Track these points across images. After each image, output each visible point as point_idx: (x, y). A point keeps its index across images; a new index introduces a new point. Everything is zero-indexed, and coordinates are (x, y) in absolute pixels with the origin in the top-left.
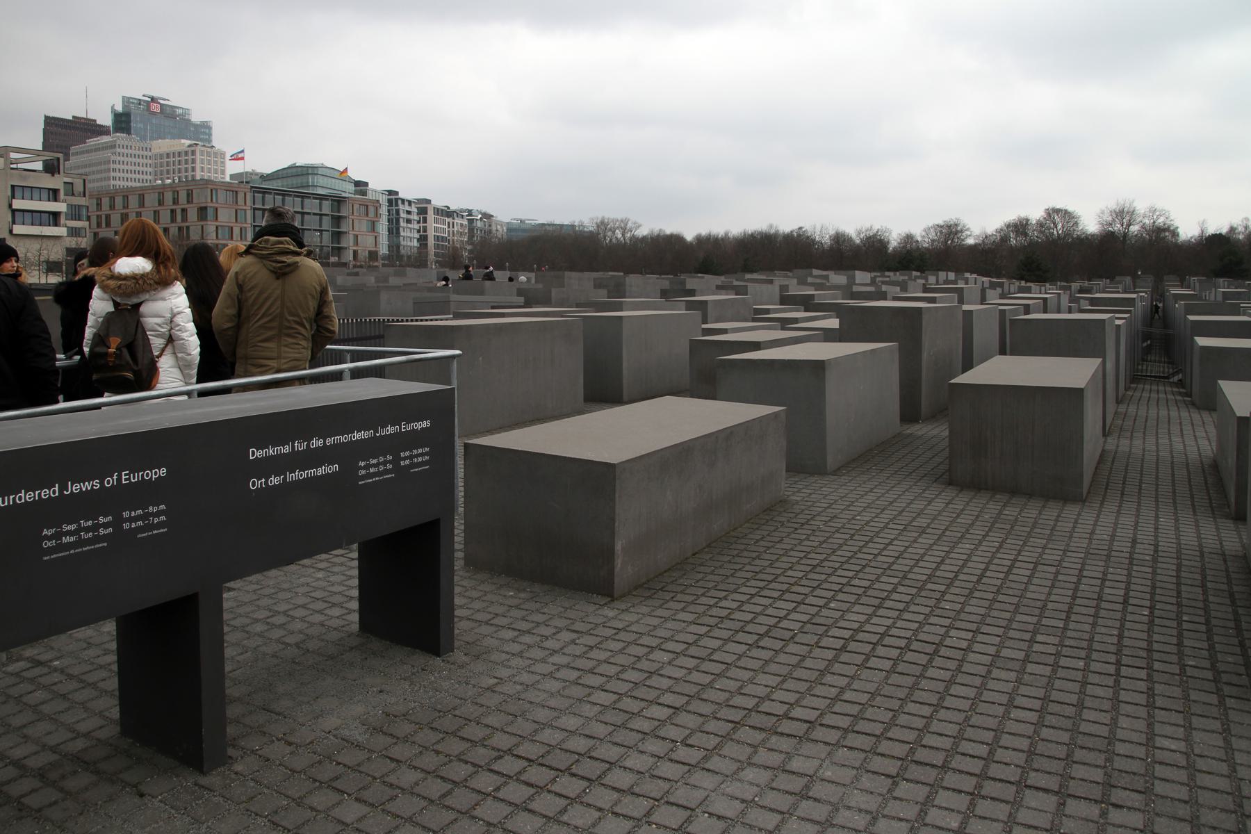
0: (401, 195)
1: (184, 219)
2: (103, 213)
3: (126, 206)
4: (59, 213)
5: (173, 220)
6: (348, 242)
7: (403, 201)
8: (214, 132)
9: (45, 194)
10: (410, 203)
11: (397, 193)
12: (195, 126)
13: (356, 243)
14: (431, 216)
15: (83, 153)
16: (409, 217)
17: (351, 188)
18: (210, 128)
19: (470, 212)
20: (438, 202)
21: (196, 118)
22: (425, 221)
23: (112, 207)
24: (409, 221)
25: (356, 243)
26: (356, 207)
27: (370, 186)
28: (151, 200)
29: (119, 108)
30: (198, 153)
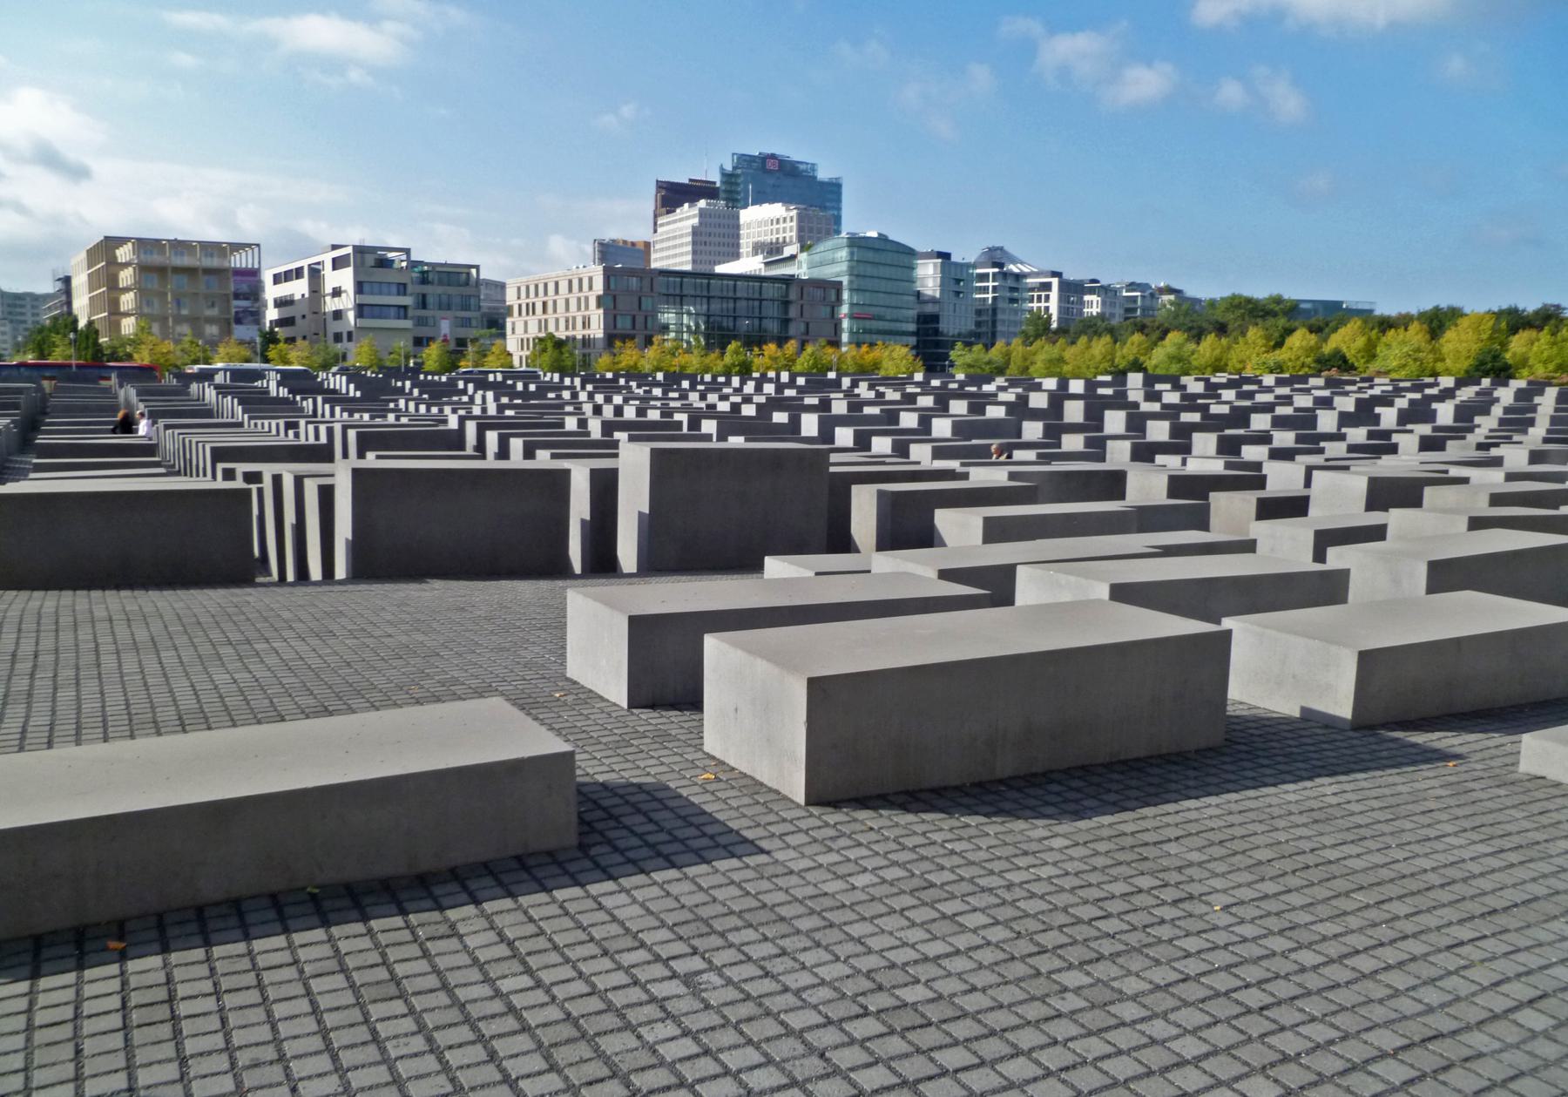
1: (587, 308)
2: (530, 301)
3: (546, 293)
4: (405, 307)
5: (579, 309)
7: (1005, 275)
9: (394, 289)
10: (1019, 277)
15: (675, 222)
19: (1132, 286)
20: (1069, 275)
21: (823, 175)
22: (1047, 298)
23: (537, 294)
24: (1013, 300)
27: (954, 259)
28: (563, 286)
29: (729, 168)
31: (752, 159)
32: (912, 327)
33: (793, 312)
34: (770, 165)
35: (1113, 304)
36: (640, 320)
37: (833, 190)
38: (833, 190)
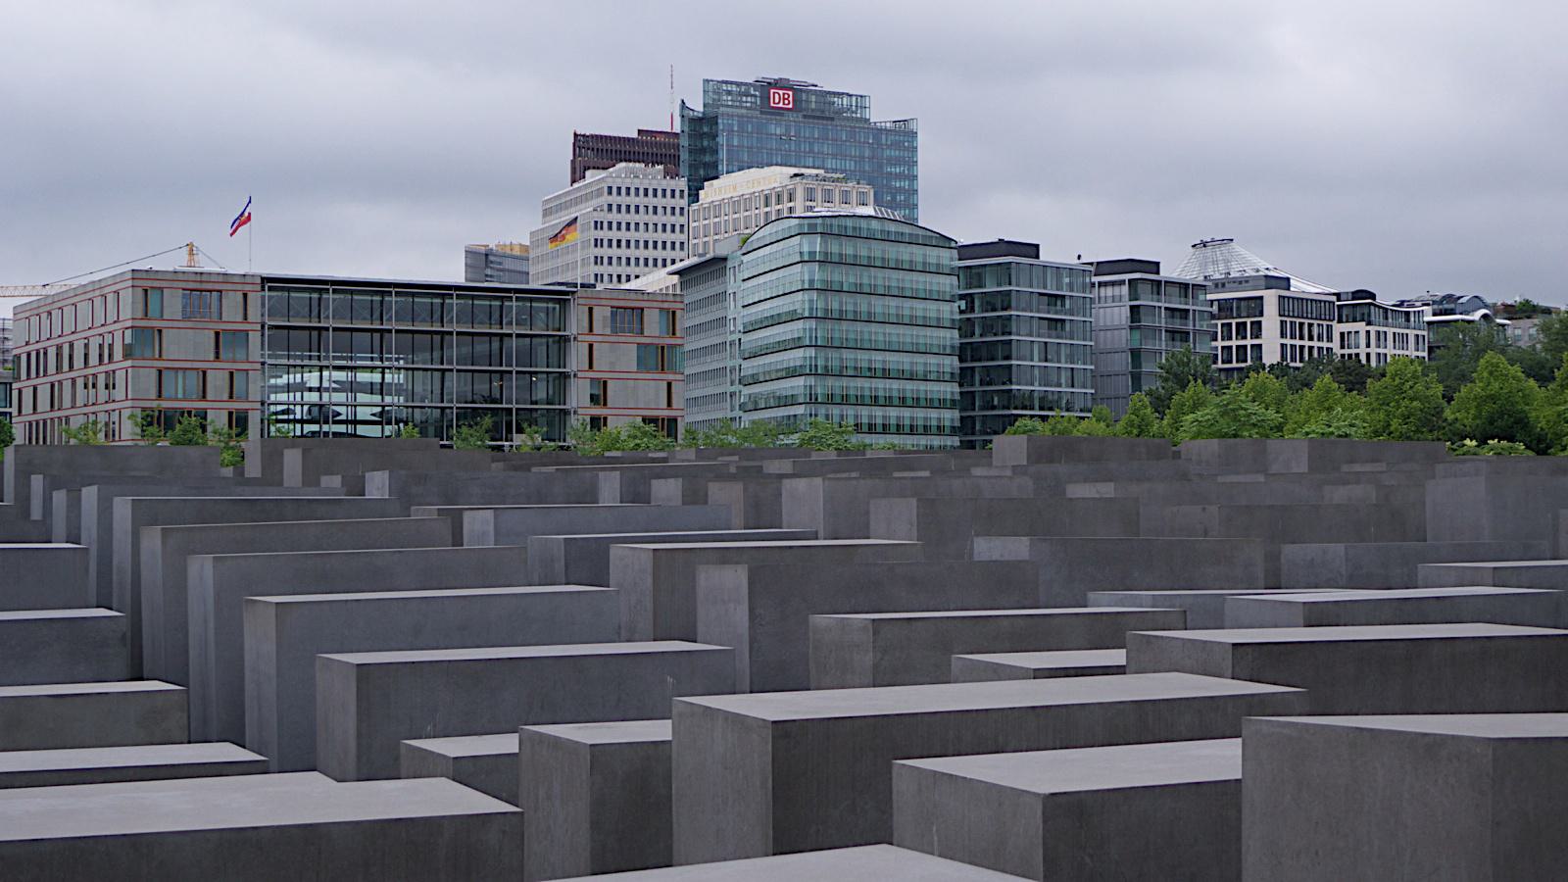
0: (1165, 273)
6: (578, 396)
8: (922, 140)
11: (1155, 267)
12: (879, 131)
13: (598, 398)
14: (1271, 321)
16: (1177, 325)
17: (947, 258)
18: (914, 135)
20: (1300, 287)
21: (880, 114)
22: (1257, 334)
25: (598, 398)
26: (602, 314)
29: (697, 105)
30: (800, 194)
31: (743, 89)
32: (951, 390)
33: (576, 359)
34: (777, 98)
35: (1401, 340)
36: (217, 381)
37: (903, 136)
38: (903, 136)
